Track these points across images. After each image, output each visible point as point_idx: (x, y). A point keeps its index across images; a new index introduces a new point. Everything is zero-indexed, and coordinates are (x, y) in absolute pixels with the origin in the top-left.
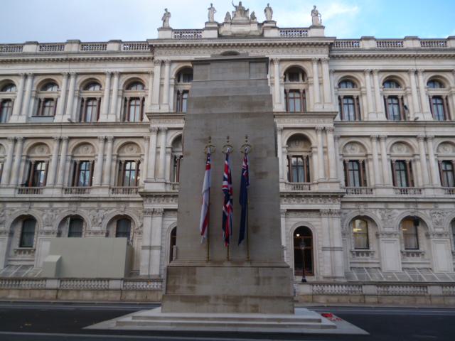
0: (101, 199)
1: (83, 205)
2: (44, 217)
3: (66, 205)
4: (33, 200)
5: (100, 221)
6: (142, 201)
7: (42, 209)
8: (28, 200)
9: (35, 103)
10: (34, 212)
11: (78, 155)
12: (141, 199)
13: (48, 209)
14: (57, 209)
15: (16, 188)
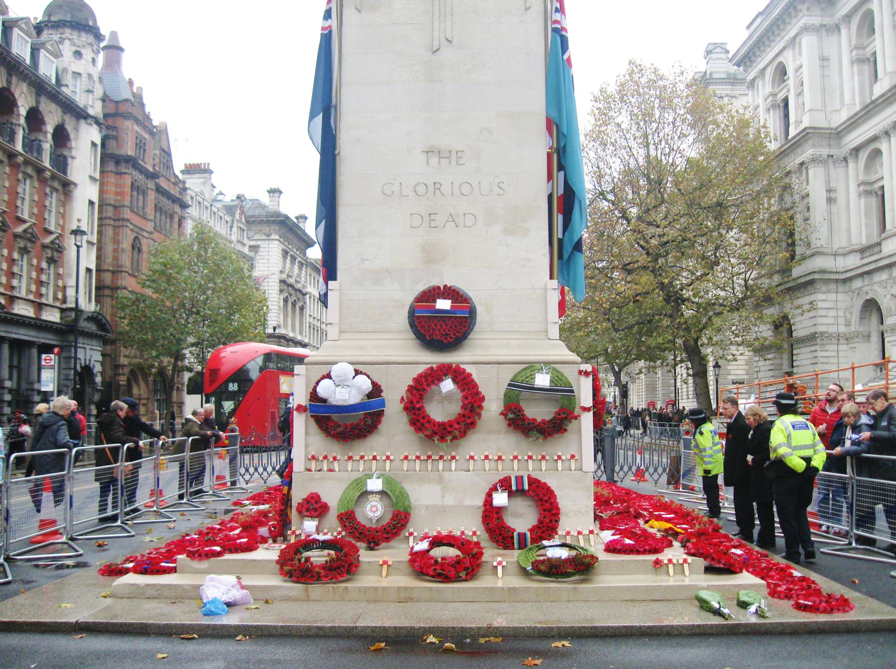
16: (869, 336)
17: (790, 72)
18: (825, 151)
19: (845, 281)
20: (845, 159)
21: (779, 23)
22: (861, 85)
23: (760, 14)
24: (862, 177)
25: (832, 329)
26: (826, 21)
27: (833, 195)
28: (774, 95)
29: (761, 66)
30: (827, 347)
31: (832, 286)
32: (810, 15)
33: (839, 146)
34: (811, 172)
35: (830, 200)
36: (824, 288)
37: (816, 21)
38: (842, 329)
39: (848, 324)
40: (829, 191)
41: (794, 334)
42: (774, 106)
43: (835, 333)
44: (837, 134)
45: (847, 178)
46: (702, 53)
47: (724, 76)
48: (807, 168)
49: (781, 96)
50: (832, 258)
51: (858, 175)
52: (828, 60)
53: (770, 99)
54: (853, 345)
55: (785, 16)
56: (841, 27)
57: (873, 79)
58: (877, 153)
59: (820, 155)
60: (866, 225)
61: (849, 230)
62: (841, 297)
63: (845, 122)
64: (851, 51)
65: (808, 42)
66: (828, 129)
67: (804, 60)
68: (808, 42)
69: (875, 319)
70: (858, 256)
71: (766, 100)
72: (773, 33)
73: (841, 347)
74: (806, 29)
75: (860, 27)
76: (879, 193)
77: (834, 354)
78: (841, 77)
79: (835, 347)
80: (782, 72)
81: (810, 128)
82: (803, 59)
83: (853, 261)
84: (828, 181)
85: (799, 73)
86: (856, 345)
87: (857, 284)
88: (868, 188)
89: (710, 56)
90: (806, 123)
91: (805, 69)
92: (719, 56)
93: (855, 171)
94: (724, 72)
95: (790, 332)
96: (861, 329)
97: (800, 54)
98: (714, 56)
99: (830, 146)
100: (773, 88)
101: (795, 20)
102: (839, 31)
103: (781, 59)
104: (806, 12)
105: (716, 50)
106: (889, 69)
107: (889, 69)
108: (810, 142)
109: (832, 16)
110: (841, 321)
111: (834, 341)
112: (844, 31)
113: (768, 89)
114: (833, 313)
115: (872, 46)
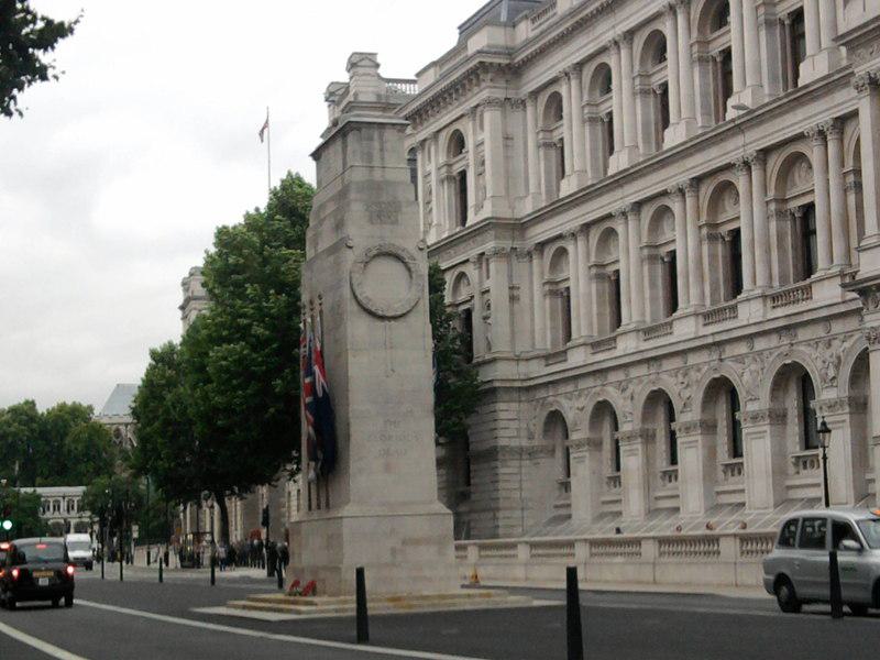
0: (824, 313)
1: (803, 334)
2: (746, 377)
3: (774, 341)
4: (724, 337)
5: (831, 373)
6: (858, 311)
7: (739, 359)
8: (710, 340)
9: (703, 75)
10: (731, 371)
11: (795, 192)
12: (860, 304)
13: (746, 355)
14: (760, 353)
15: (696, 315)
16: (553, 451)
17: (470, 144)
18: (507, 244)
19: (528, 389)
20: (529, 254)
21: (459, 86)
22: (548, 181)
23: (434, 64)
24: (547, 277)
25: (514, 443)
26: (511, 94)
27: (515, 293)
28: (449, 166)
29: (434, 128)
30: (509, 464)
31: (515, 395)
32: (495, 87)
33: (523, 237)
34: (492, 266)
35: (513, 299)
36: (506, 397)
37: (500, 94)
38: (525, 443)
39: (531, 437)
40: (511, 288)
41: (471, 447)
42: (449, 178)
43: (517, 447)
44: (520, 227)
45: (531, 273)
46: (344, 63)
47: (372, 98)
48: (487, 260)
49: (457, 168)
50: (514, 363)
51: (542, 273)
52: (512, 139)
53: (444, 170)
54: (535, 461)
55: (466, 82)
56: (528, 104)
57: (560, 174)
58: (562, 252)
59: (503, 249)
60: (552, 328)
61: (533, 331)
62: (524, 406)
63: (529, 215)
64: (538, 133)
65: (489, 116)
66: (510, 219)
67: (486, 135)
68: (489, 116)
69: (559, 433)
70: (543, 362)
71: (439, 169)
72: (450, 95)
73: (524, 463)
74: (489, 102)
75: (547, 107)
76: (565, 294)
77: (516, 471)
78: (526, 162)
79: (516, 463)
80: (458, 143)
81: (492, 218)
82: (483, 136)
83: (537, 370)
84: (510, 277)
85: (480, 150)
86: (539, 460)
87: (541, 394)
88: (554, 287)
89: (355, 70)
90: (486, 212)
91: (487, 148)
92: (368, 70)
93: (539, 267)
94: (373, 92)
95: (467, 444)
96: (544, 443)
97: (482, 127)
98: (361, 70)
99: (513, 239)
100: (448, 156)
101: (476, 89)
102: (525, 106)
103: (456, 126)
104: (491, 84)
105: (363, 63)
106: (576, 168)
107: (576, 168)
108: (492, 232)
109: (518, 88)
110: (524, 433)
111: (517, 456)
112: (530, 109)
113: (442, 159)
114: (514, 425)
115: (560, 130)
